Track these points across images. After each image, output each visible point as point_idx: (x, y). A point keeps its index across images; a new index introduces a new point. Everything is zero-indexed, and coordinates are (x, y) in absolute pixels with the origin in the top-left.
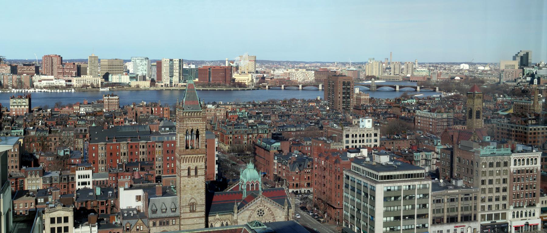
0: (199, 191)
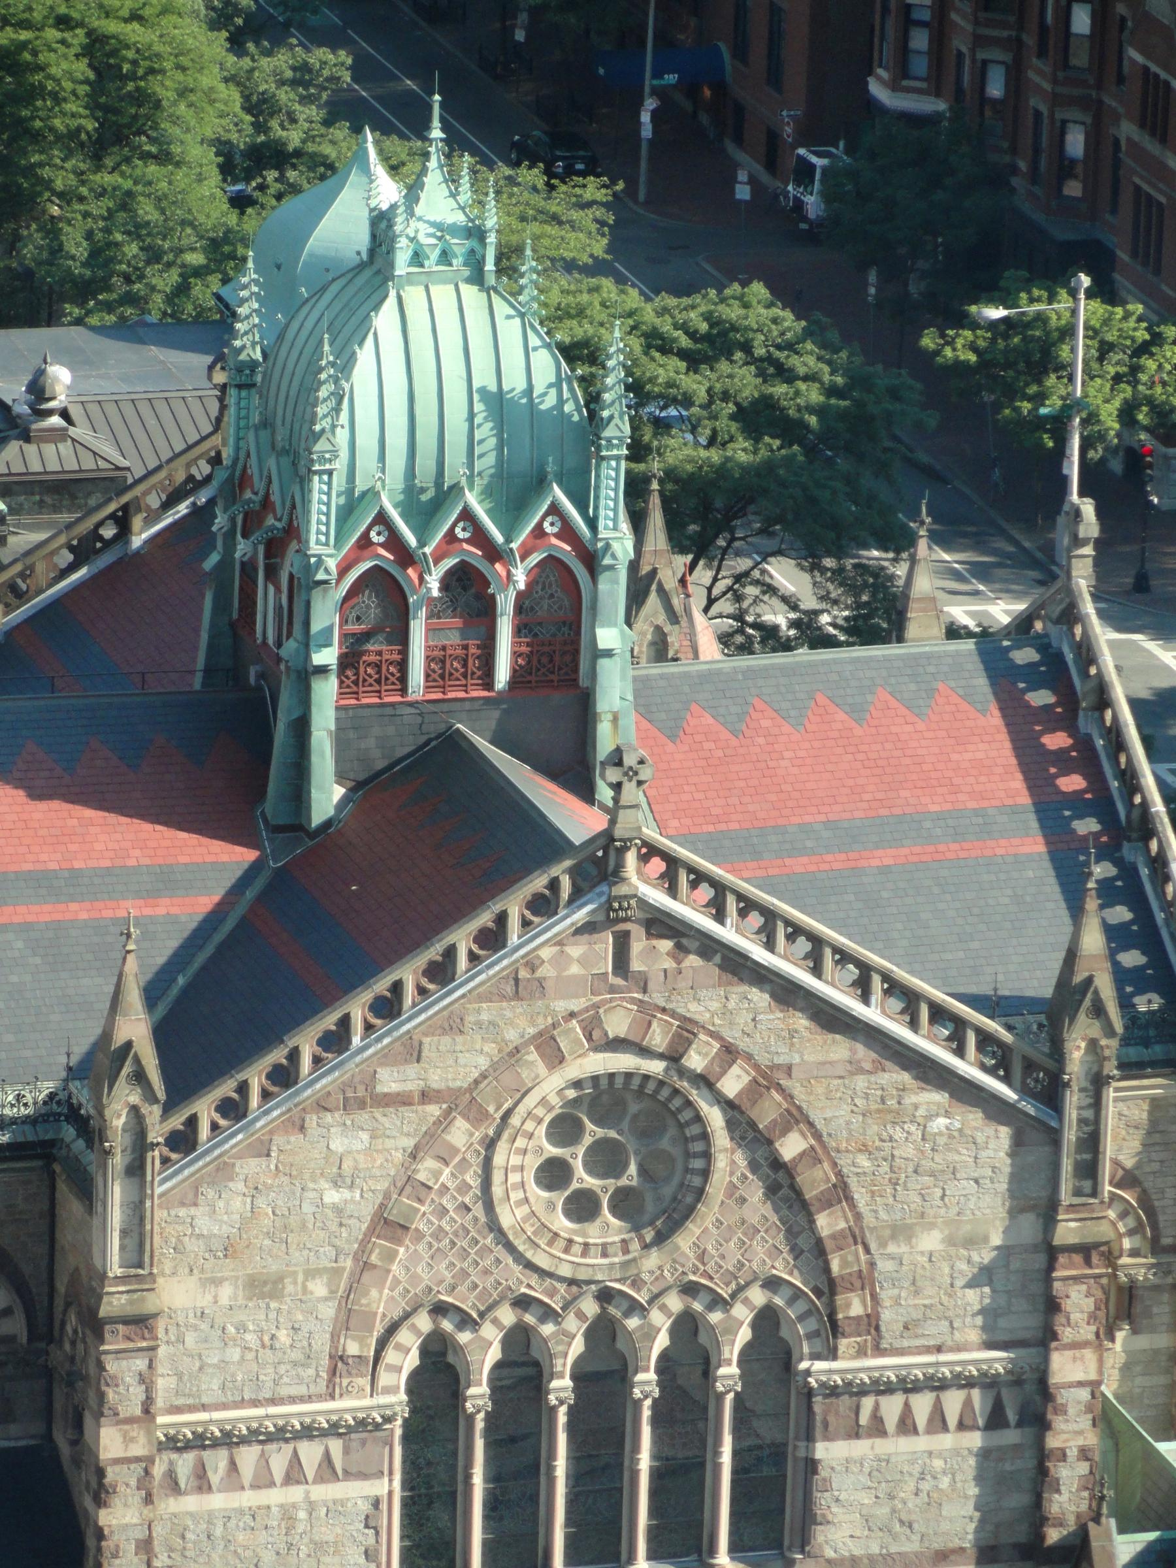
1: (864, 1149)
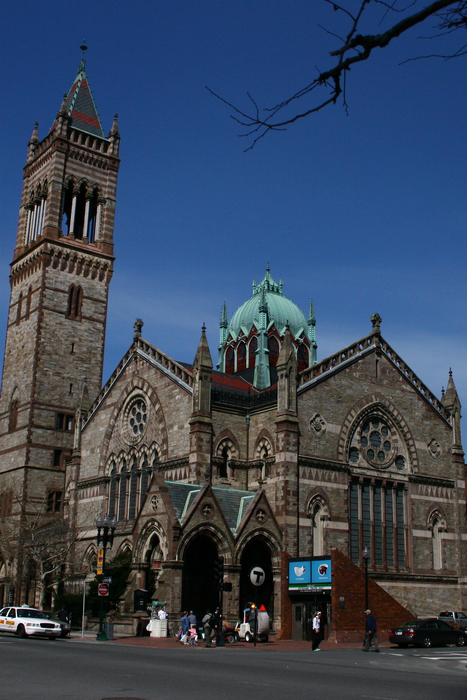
0: (27, 359)
1: (167, 406)
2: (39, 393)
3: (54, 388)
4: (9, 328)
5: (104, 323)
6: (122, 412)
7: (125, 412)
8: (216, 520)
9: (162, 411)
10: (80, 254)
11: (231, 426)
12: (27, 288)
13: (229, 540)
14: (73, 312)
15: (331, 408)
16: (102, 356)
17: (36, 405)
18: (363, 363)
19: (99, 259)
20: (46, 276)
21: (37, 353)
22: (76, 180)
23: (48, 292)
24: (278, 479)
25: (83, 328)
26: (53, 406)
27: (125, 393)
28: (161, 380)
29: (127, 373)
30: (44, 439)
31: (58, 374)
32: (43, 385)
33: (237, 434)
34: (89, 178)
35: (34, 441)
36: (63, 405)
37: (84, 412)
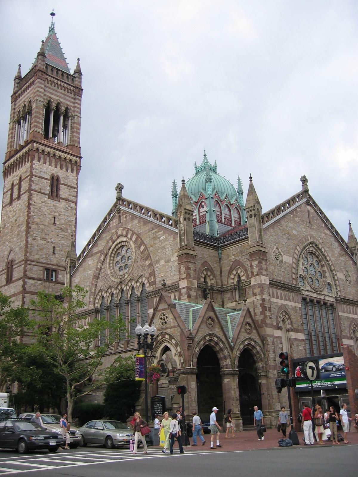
1: (152, 246)
2: (30, 253)
3: (41, 250)
4: (3, 209)
5: (76, 203)
6: (108, 257)
7: (111, 256)
8: (217, 331)
9: (148, 251)
10: (58, 153)
11: (209, 259)
12: (18, 178)
13: (228, 349)
14: (55, 194)
15: (284, 244)
16: (75, 227)
17: (28, 262)
18: (301, 211)
19: (71, 157)
20: (33, 167)
21: (28, 223)
22: (52, 101)
23: (34, 179)
24: (255, 298)
25: (61, 206)
26: (42, 263)
27: (110, 241)
28: (145, 226)
29: (111, 226)
30: (35, 288)
31: (44, 239)
32: (33, 247)
33: (213, 265)
34: (62, 100)
35: (28, 289)
36: (49, 262)
37: (73, 261)
